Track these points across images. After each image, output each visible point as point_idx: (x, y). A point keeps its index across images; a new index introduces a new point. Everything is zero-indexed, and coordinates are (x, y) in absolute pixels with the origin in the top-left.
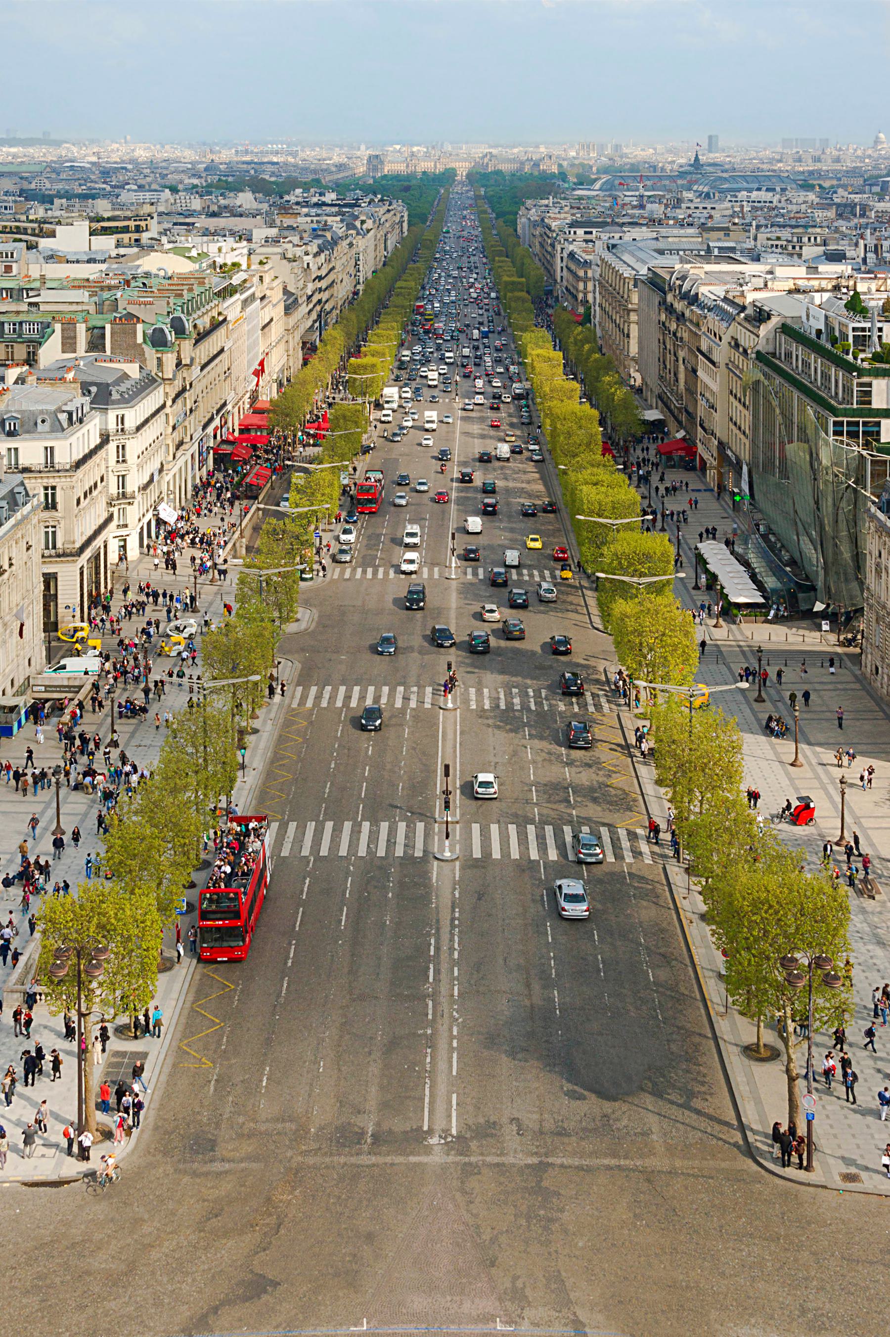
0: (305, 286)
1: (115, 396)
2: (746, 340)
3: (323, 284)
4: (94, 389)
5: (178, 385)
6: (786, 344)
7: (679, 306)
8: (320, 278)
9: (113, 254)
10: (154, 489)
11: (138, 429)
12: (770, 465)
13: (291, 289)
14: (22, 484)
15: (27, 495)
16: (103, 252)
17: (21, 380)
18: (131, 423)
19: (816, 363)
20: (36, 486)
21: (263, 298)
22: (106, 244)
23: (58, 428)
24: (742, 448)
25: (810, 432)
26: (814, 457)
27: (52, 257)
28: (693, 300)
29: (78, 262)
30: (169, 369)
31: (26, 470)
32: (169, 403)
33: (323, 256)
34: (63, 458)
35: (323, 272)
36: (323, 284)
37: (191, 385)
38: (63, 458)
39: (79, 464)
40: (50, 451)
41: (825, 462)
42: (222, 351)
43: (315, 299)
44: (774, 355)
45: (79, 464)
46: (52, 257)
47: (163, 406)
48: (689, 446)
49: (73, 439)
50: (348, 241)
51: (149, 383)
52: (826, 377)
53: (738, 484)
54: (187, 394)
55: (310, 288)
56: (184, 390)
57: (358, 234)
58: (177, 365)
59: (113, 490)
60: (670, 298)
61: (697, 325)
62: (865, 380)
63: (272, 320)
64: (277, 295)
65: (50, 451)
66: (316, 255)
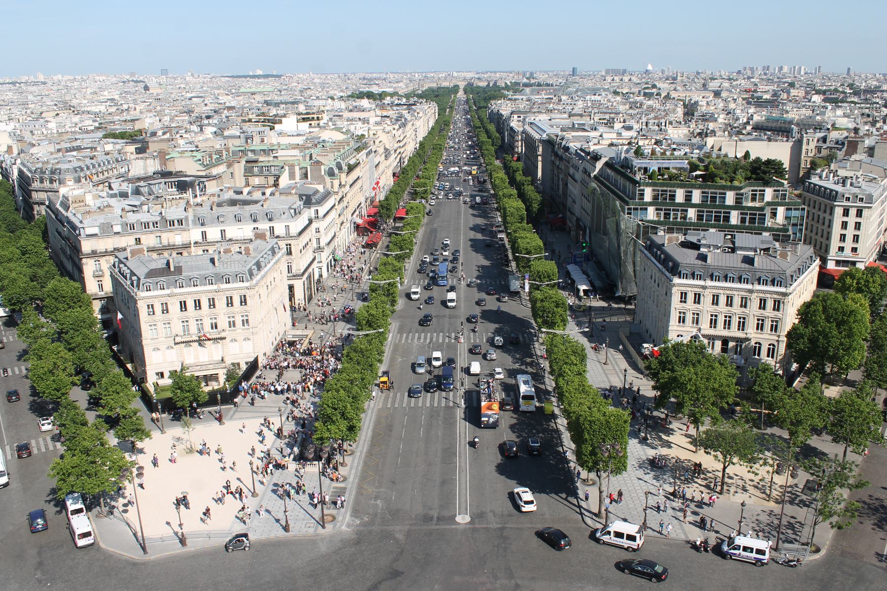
1: (314, 201)
3: (401, 144)
4: (304, 198)
8: (399, 141)
10: (332, 243)
11: (325, 216)
12: (599, 228)
17: (272, 194)
18: (321, 214)
30: (336, 189)
31: (278, 237)
34: (294, 231)
36: (401, 144)
39: (300, 233)
40: (287, 227)
47: (334, 205)
48: (564, 220)
51: (327, 195)
53: (584, 237)
55: (396, 145)
56: (343, 197)
65: (287, 227)
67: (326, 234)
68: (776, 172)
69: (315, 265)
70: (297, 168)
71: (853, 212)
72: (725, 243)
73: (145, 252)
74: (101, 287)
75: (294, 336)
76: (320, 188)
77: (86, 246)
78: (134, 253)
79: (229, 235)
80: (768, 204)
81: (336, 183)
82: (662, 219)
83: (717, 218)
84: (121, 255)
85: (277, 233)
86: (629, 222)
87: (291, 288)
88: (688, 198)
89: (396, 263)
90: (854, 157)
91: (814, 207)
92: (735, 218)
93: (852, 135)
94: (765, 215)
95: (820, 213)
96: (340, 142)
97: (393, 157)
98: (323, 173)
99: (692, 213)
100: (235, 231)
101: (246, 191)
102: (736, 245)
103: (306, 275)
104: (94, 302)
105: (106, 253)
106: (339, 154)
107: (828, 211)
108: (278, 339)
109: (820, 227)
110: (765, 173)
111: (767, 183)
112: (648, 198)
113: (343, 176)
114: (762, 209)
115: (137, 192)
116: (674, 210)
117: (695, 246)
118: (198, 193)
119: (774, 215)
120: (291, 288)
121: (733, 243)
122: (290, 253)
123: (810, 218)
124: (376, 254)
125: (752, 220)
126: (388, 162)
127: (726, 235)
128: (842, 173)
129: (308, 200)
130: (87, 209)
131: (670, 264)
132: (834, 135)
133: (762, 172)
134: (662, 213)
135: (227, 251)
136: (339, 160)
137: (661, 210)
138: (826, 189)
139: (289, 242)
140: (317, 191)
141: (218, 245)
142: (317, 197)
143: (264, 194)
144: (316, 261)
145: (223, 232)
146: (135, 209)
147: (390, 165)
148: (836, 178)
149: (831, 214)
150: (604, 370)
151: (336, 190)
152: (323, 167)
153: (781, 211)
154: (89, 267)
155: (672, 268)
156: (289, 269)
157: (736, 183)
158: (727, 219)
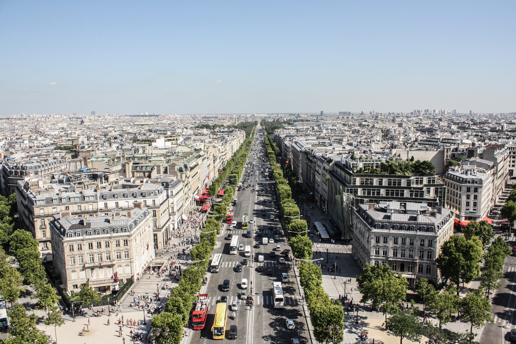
2: (327, 167)
6: (336, 168)
7: (311, 158)
19: (343, 173)
23: (156, 195)
24: (326, 196)
25: (341, 191)
26: (342, 198)
28: (314, 157)
34: (158, 203)
38: (158, 203)
39: (161, 204)
41: (344, 200)
44: (333, 171)
45: (161, 204)
49: (159, 198)
52: (345, 177)
59: (171, 211)
60: (309, 156)
61: (315, 163)
62: (355, 178)
68: (428, 168)
71: (472, 189)
72: (400, 208)
73: (70, 215)
74: (45, 235)
75: (156, 264)
77: (37, 211)
78: (63, 215)
79: (120, 205)
80: (425, 185)
82: (366, 195)
83: (397, 194)
84: (57, 217)
85: (148, 204)
86: (346, 197)
87: (155, 235)
88: (381, 183)
89: (215, 221)
90: (472, 159)
91: (451, 187)
92: (407, 194)
93: (471, 147)
94: (423, 192)
95: (454, 190)
99: (383, 192)
100: (123, 203)
102: (407, 209)
103: (165, 228)
104: (40, 244)
105: (48, 216)
107: (459, 189)
108: (146, 265)
109: (455, 198)
110: (423, 168)
111: (423, 174)
112: (358, 183)
114: (422, 188)
116: (373, 190)
117: (384, 210)
118: (103, 181)
119: (429, 192)
120: (155, 235)
121: (405, 208)
122: (155, 215)
123: (450, 193)
124: (204, 217)
125: (416, 195)
127: (401, 203)
128: (466, 167)
130: (39, 189)
131: (370, 220)
132: (461, 147)
133: (420, 169)
134: (366, 191)
135: (117, 214)
137: (365, 190)
138: (457, 176)
139: (155, 209)
144: (171, 220)
145: (117, 204)
146: (67, 190)
148: (462, 171)
149: (460, 191)
150: (334, 282)
153: (432, 189)
154: (38, 223)
155: (371, 223)
157: (407, 175)
158: (402, 194)
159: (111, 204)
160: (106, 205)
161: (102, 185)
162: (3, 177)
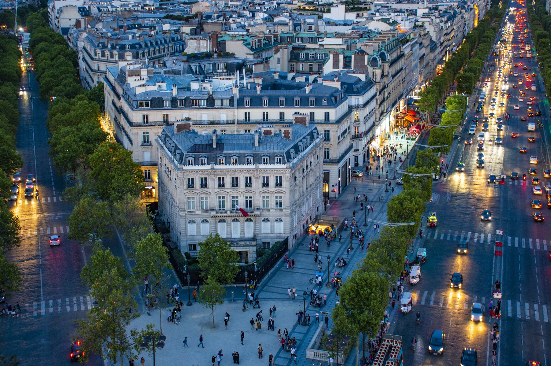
0: (440, 38)
5: (382, 84)
8: (447, 34)
9: (355, 21)
13: (434, 39)
14: (316, 129)
15: (318, 134)
16: (351, 21)
20: (321, 129)
21: (421, 44)
22: (352, 16)
27: (328, 23)
29: (339, 25)
30: (378, 79)
32: (378, 94)
33: (449, 22)
35: (449, 31)
36: (448, 37)
37: (388, 85)
40: (327, 115)
42: (401, 69)
43: (444, 45)
46: (328, 23)
47: (375, 95)
50: (461, 16)
51: (370, 83)
54: (386, 90)
57: (466, 11)
58: (383, 76)
63: (424, 55)
64: (426, 42)
65: (327, 115)
66: (446, 22)
67: (365, 123)
69: (351, 154)
70: (341, 57)
76: (363, 77)
81: (378, 72)
96: (386, 33)
97: (439, 50)
98: (366, 63)
101: (290, 76)
106: (383, 45)
113: (386, 66)
115: (190, 71)
122: (327, 138)
126: (432, 56)
129: (351, 89)
136: (383, 51)
140: (359, 80)
141: (260, 126)
142: (359, 86)
143: (307, 80)
144: (353, 149)
147: (435, 58)
151: (378, 79)
152: (366, 57)
156: (327, 155)
159: (256, 114)
160: (247, 115)
161: (242, 82)
162: (84, 59)
